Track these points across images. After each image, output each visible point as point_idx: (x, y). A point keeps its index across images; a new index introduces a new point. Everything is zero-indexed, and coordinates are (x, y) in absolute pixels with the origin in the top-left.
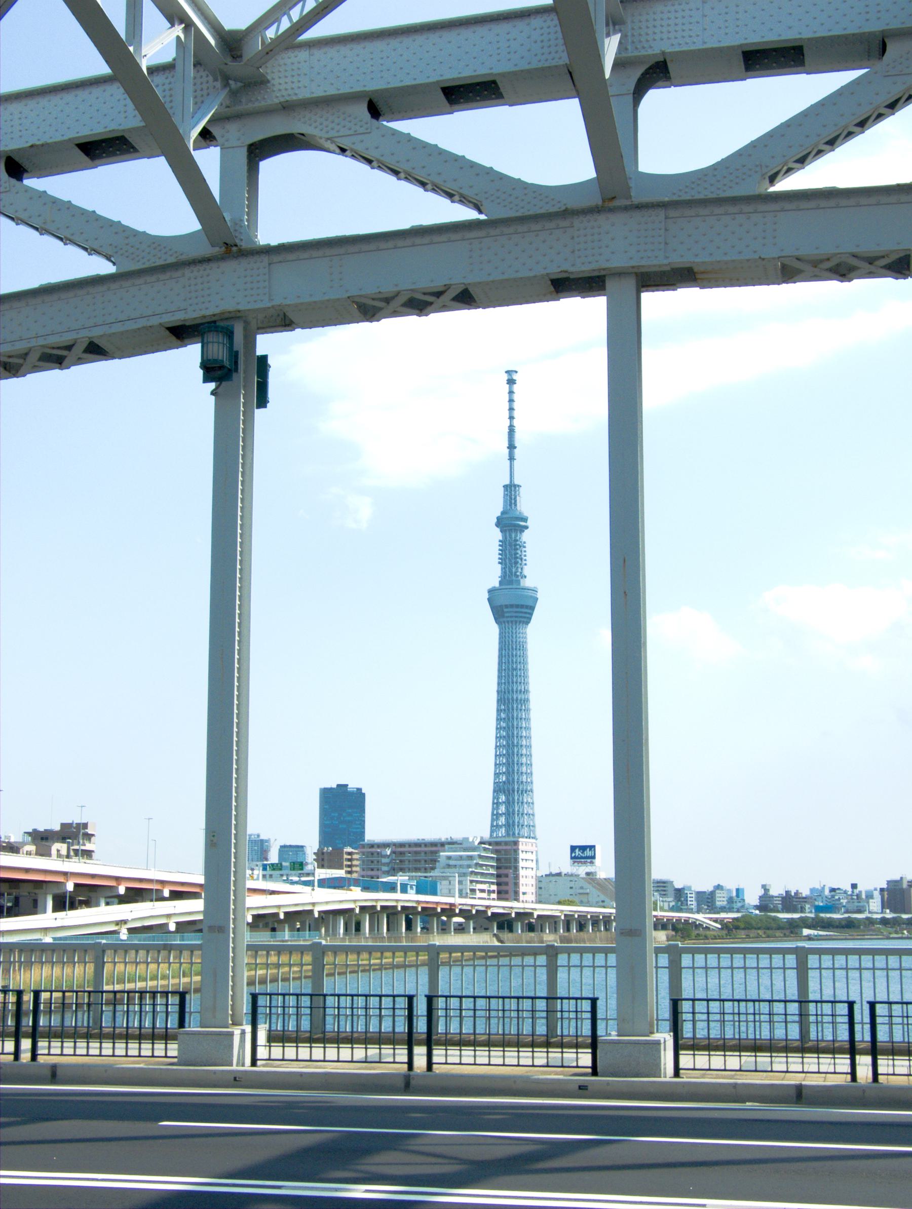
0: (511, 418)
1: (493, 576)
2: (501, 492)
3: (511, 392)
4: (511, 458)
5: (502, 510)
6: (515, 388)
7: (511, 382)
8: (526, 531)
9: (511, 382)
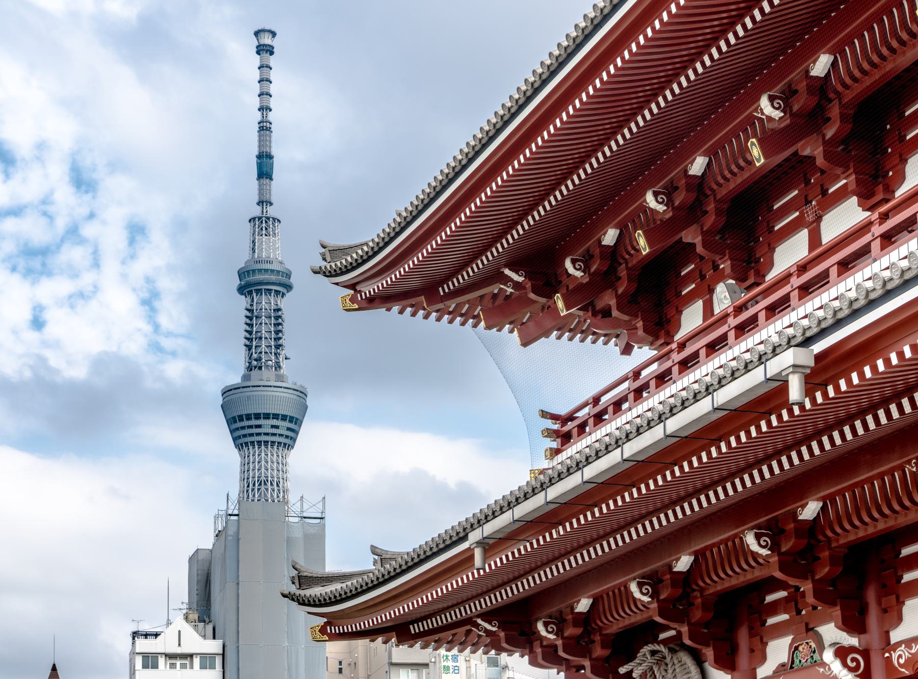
7: (264, 50)
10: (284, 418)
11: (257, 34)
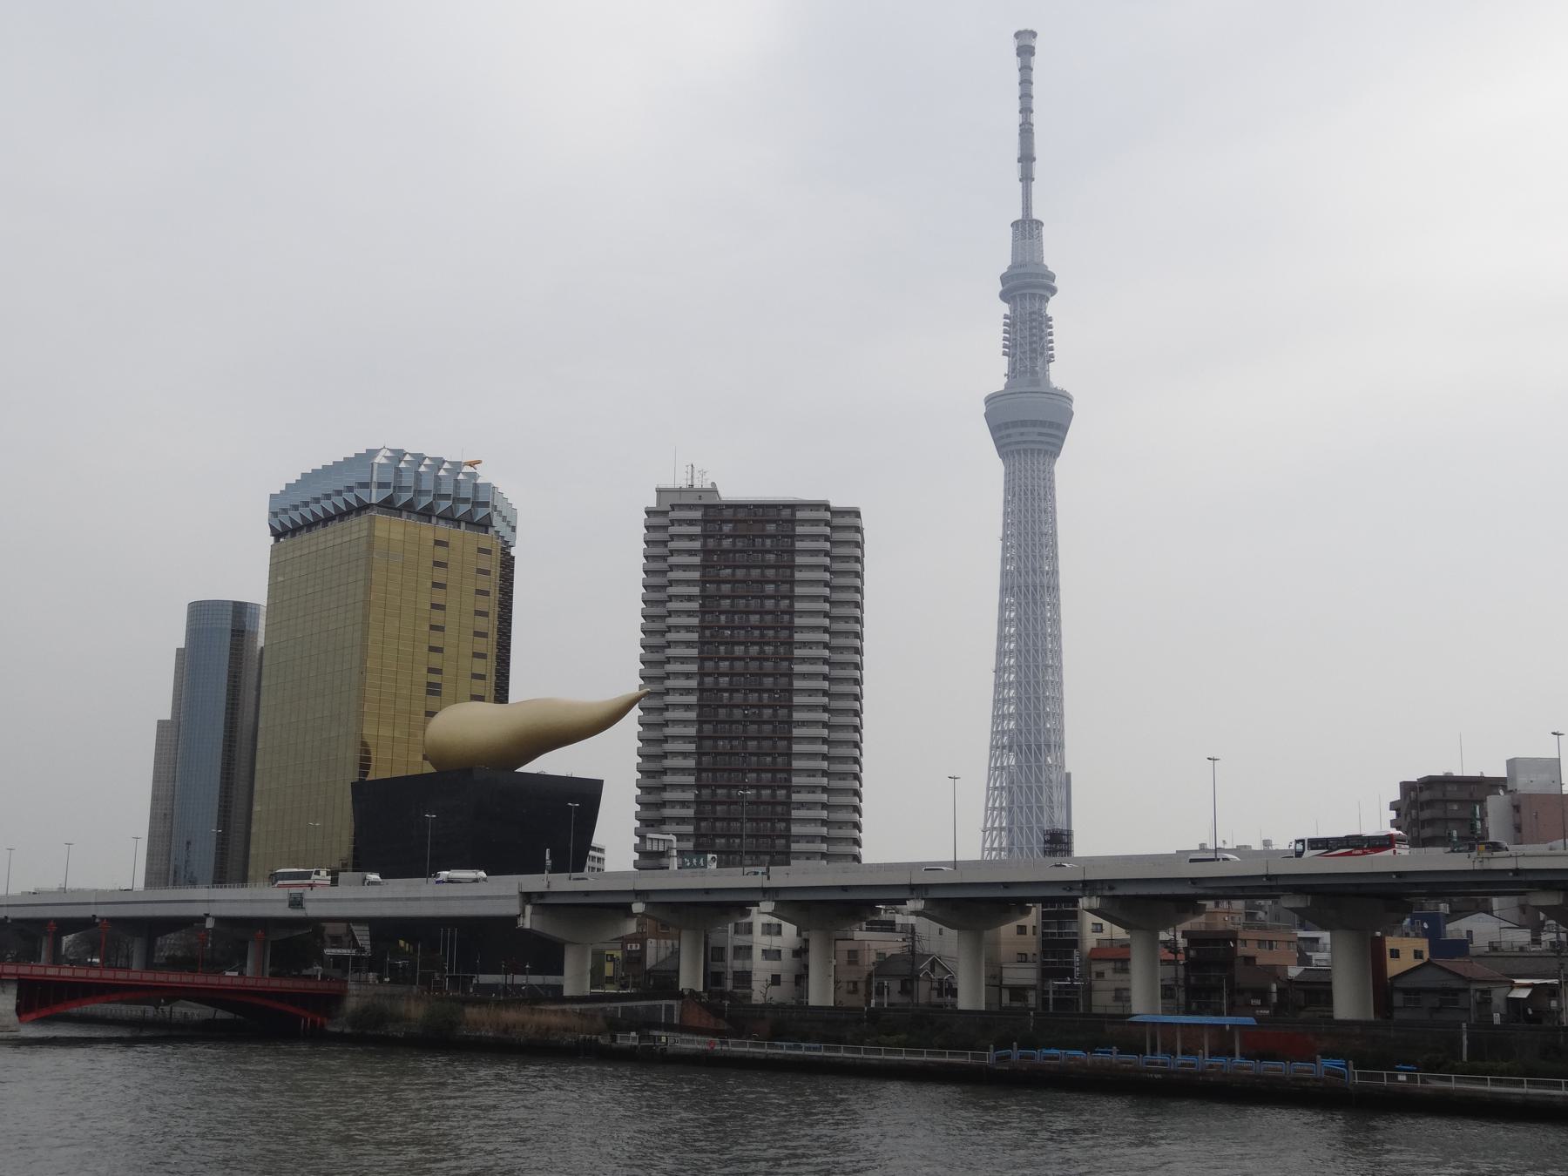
0: (1026, 110)
1: (994, 374)
2: (1007, 234)
3: (1026, 69)
4: (1027, 178)
5: (1009, 263)
6: (1037, 62)
7: (1025, 47)
8: (1052, 299)
9: (1025, 47)
10: (1034, 423)
11: (1018, 35)
